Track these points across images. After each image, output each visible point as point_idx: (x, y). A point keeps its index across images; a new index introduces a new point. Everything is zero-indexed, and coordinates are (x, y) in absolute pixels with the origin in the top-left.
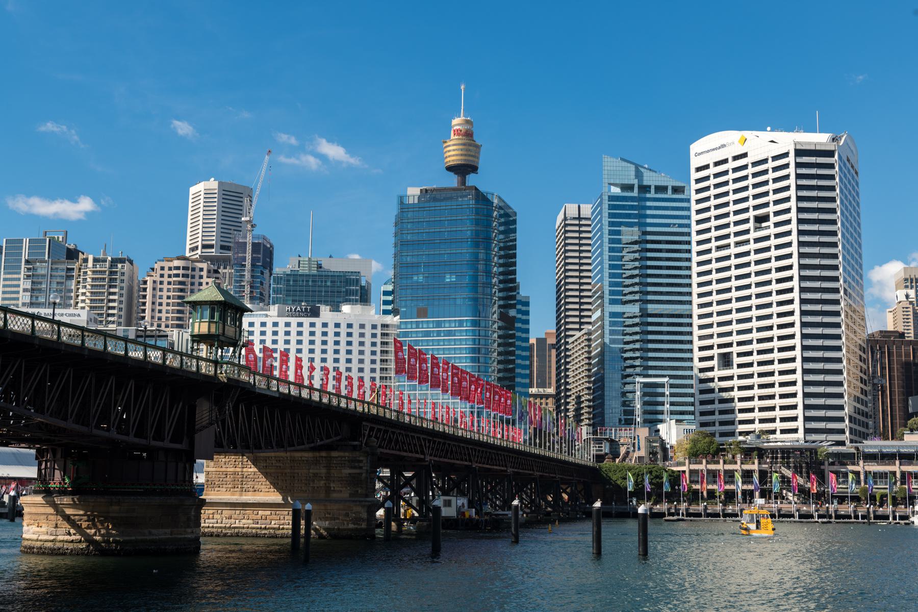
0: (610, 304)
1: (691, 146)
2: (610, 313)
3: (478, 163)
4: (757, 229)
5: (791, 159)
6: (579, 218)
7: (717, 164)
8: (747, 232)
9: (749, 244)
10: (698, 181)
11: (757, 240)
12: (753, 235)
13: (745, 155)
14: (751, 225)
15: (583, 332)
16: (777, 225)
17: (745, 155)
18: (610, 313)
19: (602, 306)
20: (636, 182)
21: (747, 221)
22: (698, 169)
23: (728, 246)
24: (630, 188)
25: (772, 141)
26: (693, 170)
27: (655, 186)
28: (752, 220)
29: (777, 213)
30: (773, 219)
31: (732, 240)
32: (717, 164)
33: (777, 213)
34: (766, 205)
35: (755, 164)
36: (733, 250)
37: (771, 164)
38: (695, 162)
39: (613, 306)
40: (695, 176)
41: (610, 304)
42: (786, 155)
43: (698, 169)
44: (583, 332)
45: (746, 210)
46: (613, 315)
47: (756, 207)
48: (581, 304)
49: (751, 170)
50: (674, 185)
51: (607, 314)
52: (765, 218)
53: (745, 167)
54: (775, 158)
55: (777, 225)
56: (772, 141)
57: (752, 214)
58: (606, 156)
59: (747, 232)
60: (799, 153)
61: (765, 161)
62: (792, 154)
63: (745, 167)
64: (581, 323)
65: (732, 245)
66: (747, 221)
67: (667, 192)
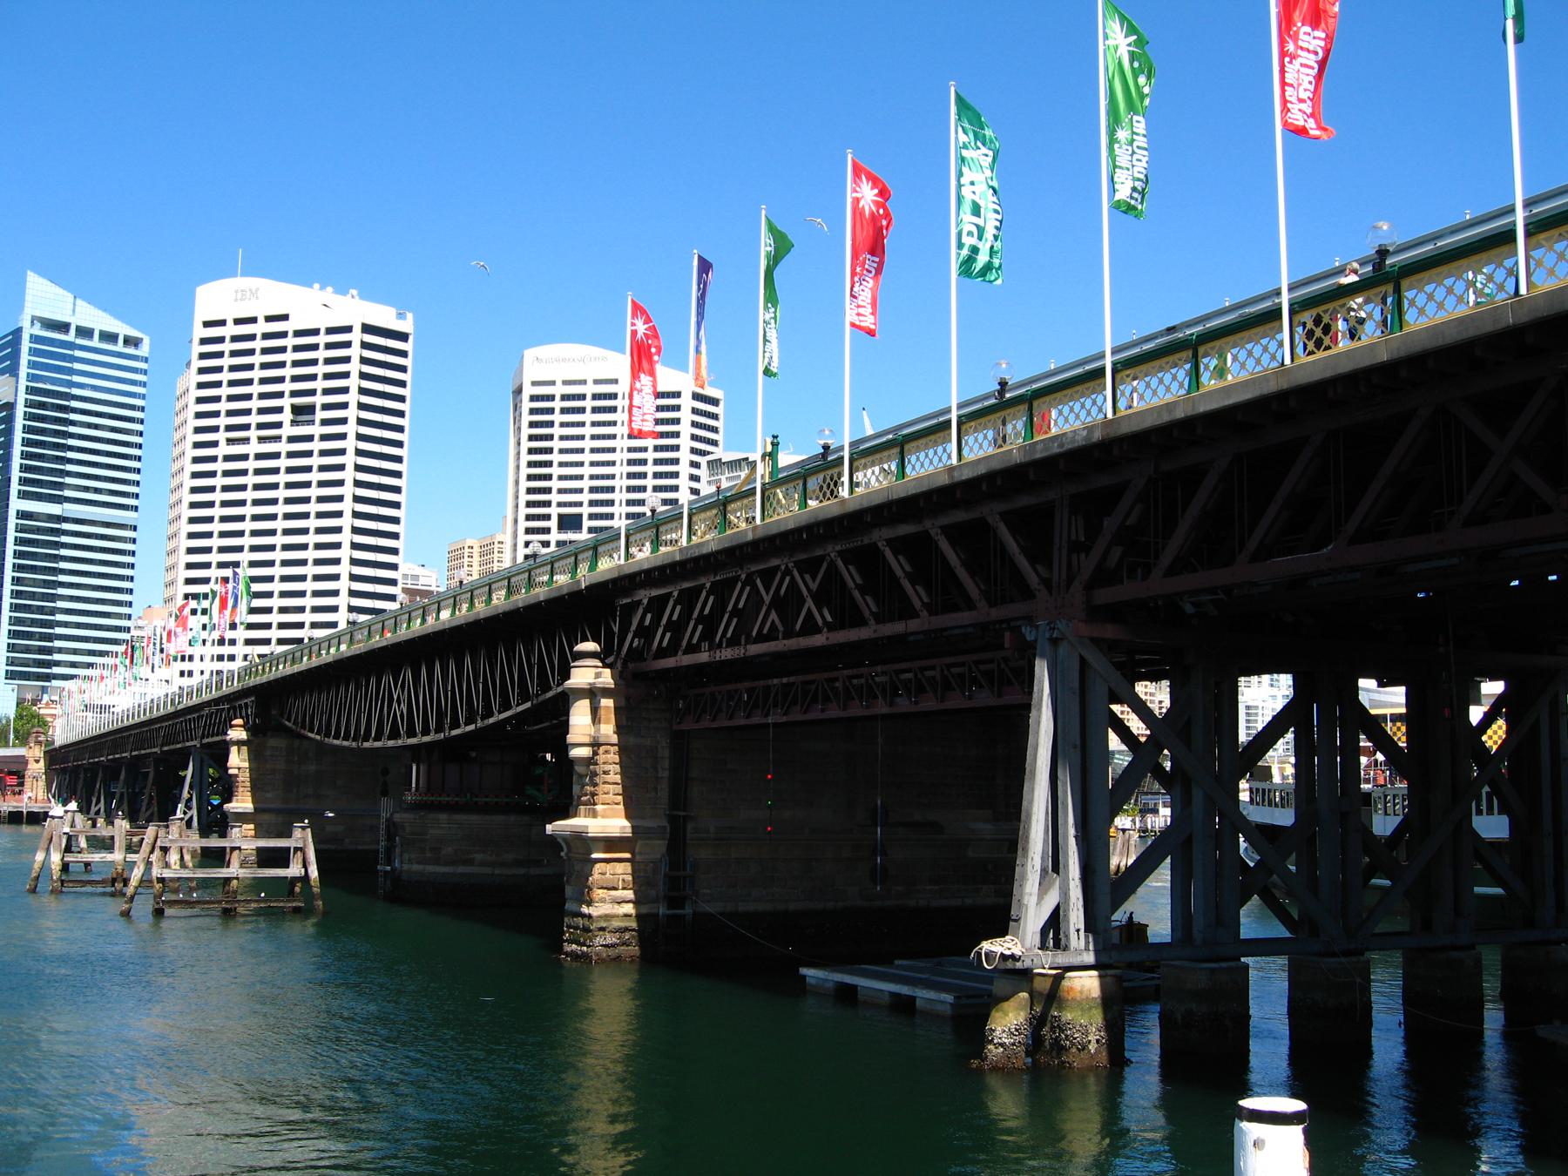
0: (18, 498)
4: (294, 423)
5: (356, 337)
7: (238, 322)
8: (279, 425)
9: (280, 441)
10: (204, 341)
11: (292, 439)
12: (288, 430)
13: (285, 317)
14: (287, 416)
16: (325, 422)
17: (285, 317)
18: (18, 511)
21: (279, 410)
22: (207, 324)
23: (246, 440)
24: (64, 327)
25: (325, 305)
26: (198, 325)
28: (288, 410)
29: (326, 407)
30: (320, 415)
31: (253, 434)
32: (238, 322)
33: (326, 407)
34: (312, 392)
35: (298, 334)
36: (254, 448)
37: (322, 339)
38: (202, 314)
40: (202, 332)
41: (18, 498)
42: (348, 329)
43: (207, 324)
45: (280, 395)
46: (23, 515)
47: (294, 394)
49: (290, 342)
52: (310, 409)
53: (283, 335)
54: (330, 331)
55: (325, 422)
56: (325, 305)
57: (286, 402)
59: (279, 425)
60: (367, 329)
61: (315, 332)
62: (357, 329)
63: (283, 335)
65: (254, 440)
66: (279, 410)
67: (117, 342)
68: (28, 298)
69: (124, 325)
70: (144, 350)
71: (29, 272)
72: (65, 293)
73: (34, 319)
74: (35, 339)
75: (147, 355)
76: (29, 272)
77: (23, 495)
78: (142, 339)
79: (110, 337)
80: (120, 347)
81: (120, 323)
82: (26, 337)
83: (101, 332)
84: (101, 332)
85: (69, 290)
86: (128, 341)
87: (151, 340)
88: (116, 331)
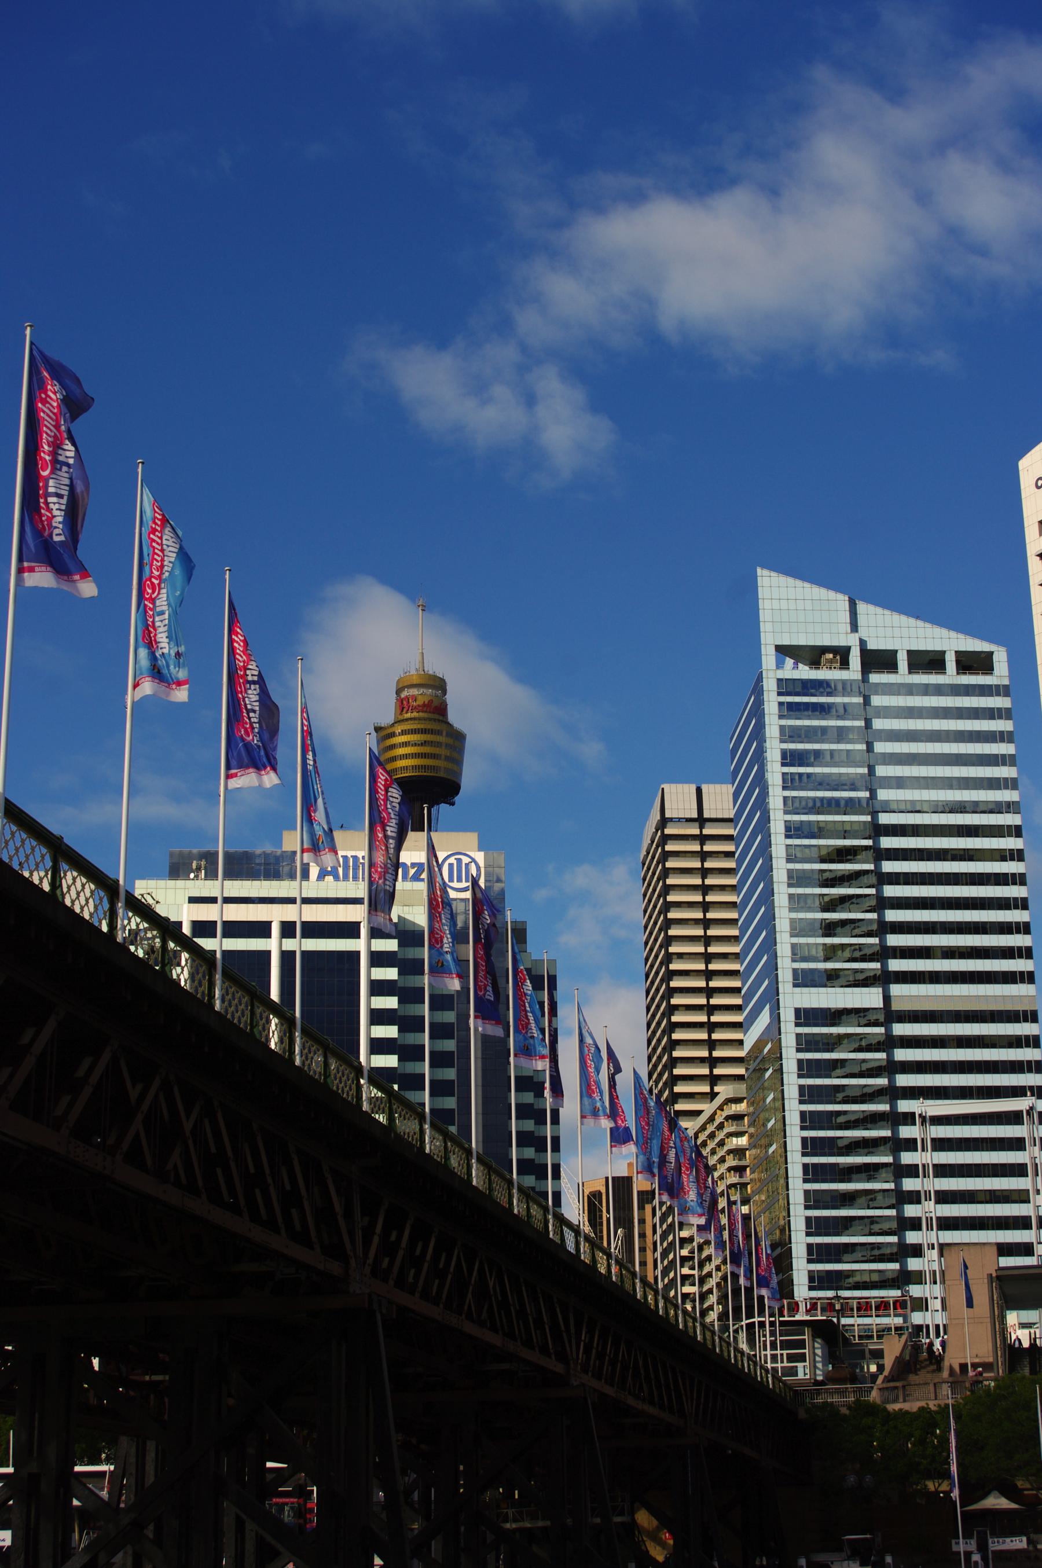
0: (795, 985)
1: (1023, 464)
2: (797, 1011)
3: (459, 774)
6: (701, 820)
15: (718, 1101)
18: (797, 1011)
19: (773, 998)
20: (852, 641)
27: (909, 652)
39: (805, 990)
44: (718, 1101)
46: (805, 1016)
48: (712, 1044)
50: (962, 649)
51: (787, 1016)
58: (766, 572)
64: (714, 1080)
68: (764, 615)
69: (953, 634)
70: (1001, 672)
71: (759, 570)
72: (832, 594)
73: (783, 651)
74: (786, 687)
75: (1006, 682)
76: (759, 570)
77: (804, 980)
78: (991, 653)
79: (932, 661)
80: (951, 675)
81: (945, 632)
82: (770, 686)
83: (910, 653)
84: (910, 653)
85: (837, 589)
86: (970, 662)
87: (1008, 652)
88: (938, 648)
